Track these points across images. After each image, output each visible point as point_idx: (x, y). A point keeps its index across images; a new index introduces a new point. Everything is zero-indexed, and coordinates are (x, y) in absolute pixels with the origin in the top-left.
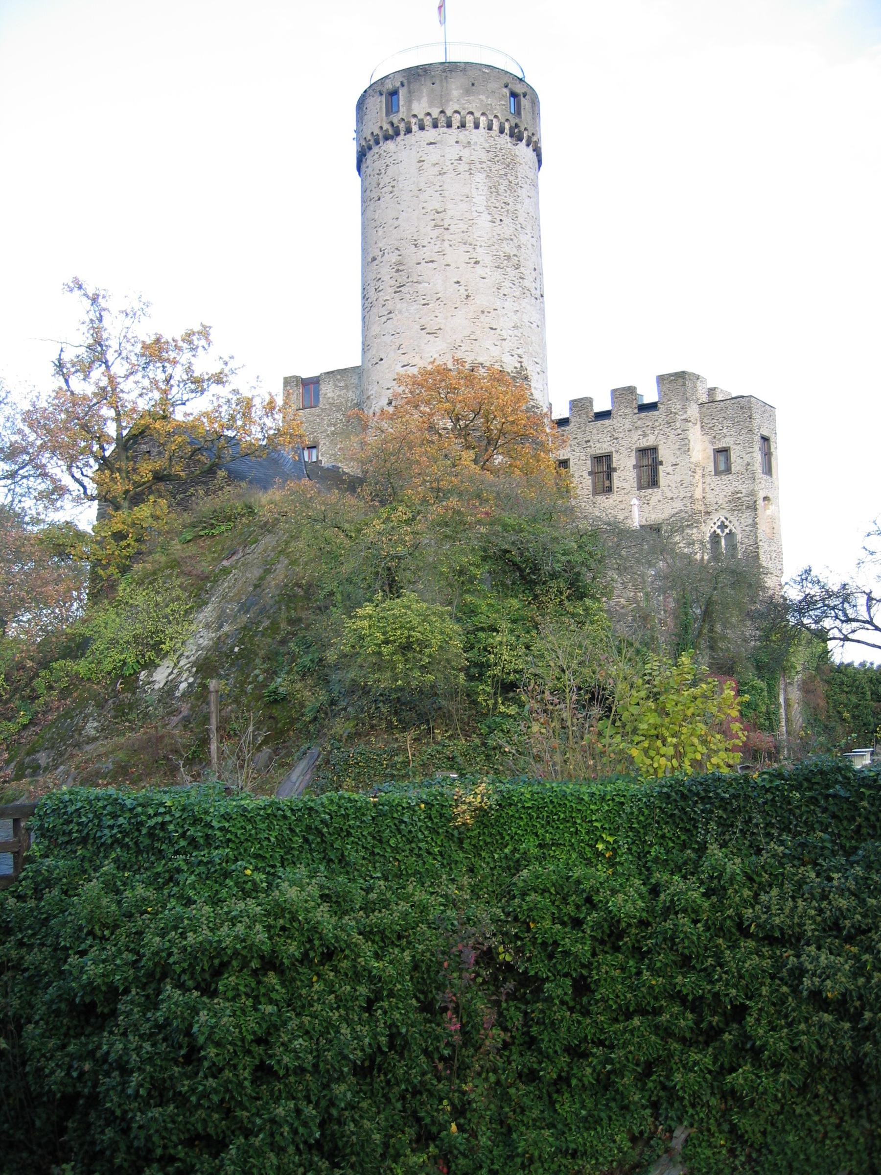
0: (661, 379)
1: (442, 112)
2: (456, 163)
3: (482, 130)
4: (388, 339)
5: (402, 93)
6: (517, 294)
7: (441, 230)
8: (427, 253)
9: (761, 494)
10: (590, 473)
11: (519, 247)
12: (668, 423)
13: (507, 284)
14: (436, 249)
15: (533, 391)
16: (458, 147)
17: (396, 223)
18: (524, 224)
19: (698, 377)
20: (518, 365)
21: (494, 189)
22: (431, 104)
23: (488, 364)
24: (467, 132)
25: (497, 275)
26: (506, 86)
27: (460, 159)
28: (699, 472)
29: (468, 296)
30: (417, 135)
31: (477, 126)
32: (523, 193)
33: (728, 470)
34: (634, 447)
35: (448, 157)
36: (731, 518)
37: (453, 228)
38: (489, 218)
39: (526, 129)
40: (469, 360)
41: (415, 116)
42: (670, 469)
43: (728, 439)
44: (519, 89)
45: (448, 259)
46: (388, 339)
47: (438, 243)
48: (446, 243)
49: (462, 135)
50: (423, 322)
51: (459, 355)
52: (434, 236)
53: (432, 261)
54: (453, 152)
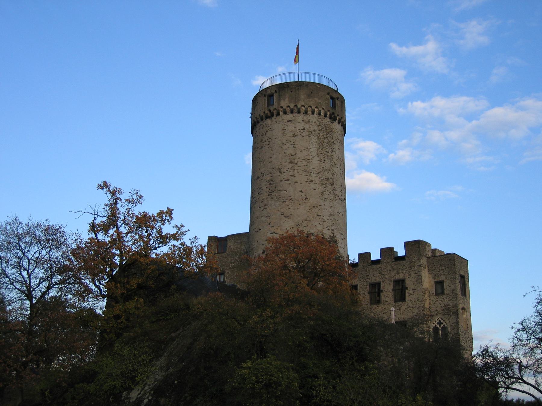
0: (407, 245)
1: (296, 106)
2: (302, 131)
3: (315, 115)
4: (264, 219)
5: (276, 96)
6: (332, 198)
7: (293, 165)
8: (286, 176)
9: (461, 306)
10: (369, 293)
11: (333, 174)
12: (411, 267)
13: (327, 193)
14: (291, 173)
15: (339, 248)
16: (303, 123)
17: (270, 160)
18: (336, 162)
19: (426, 243)
20: (332, 235)
21: (321, 145)
22: (290, 102)
23: (316, 234)
24: (308, 116)
25: (322, 188)
26: (328, 94)
27: (304, 129)
28: (427, 294)
29: (306, 198)
30: (283, 117)
31: (313, 113)
32: (336, 147)
33: (443, 293)
34: (392, 279)
35: (298, 128)
36: (445, 319)
37: (299, 163)
38: (318, 159)
39: (338, 115)
40: (306, 231)
41: (282, 107)
42: (411, 292)
43: (442, 276)
44: (335, 95)
45: (297, 179)
46: (264, 219)
47: (292, 171)
48: (296, 171)
49: (306, 118)
50: (282, 210)
51: (301, 228)
52: (290, 167)
53: (288, 180)
54: (300, 126)
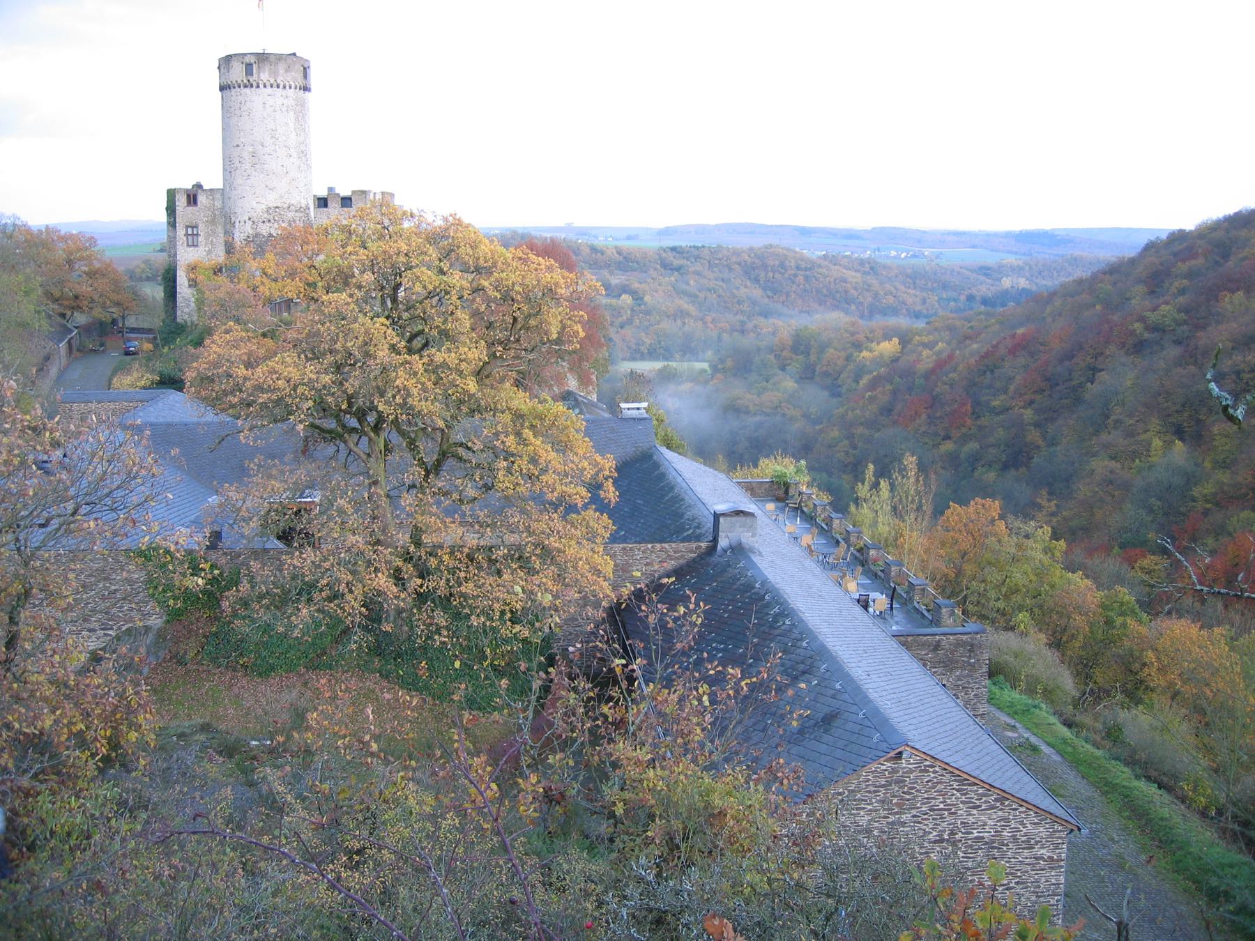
21: (297, 119)
49: (284, 93)
